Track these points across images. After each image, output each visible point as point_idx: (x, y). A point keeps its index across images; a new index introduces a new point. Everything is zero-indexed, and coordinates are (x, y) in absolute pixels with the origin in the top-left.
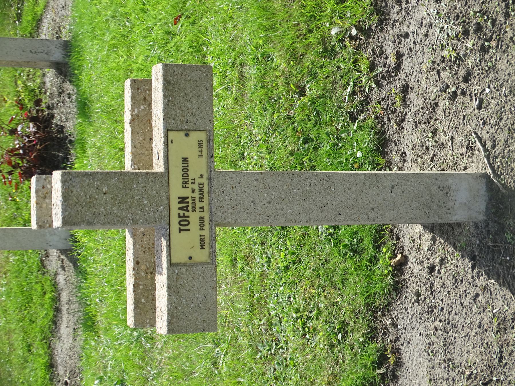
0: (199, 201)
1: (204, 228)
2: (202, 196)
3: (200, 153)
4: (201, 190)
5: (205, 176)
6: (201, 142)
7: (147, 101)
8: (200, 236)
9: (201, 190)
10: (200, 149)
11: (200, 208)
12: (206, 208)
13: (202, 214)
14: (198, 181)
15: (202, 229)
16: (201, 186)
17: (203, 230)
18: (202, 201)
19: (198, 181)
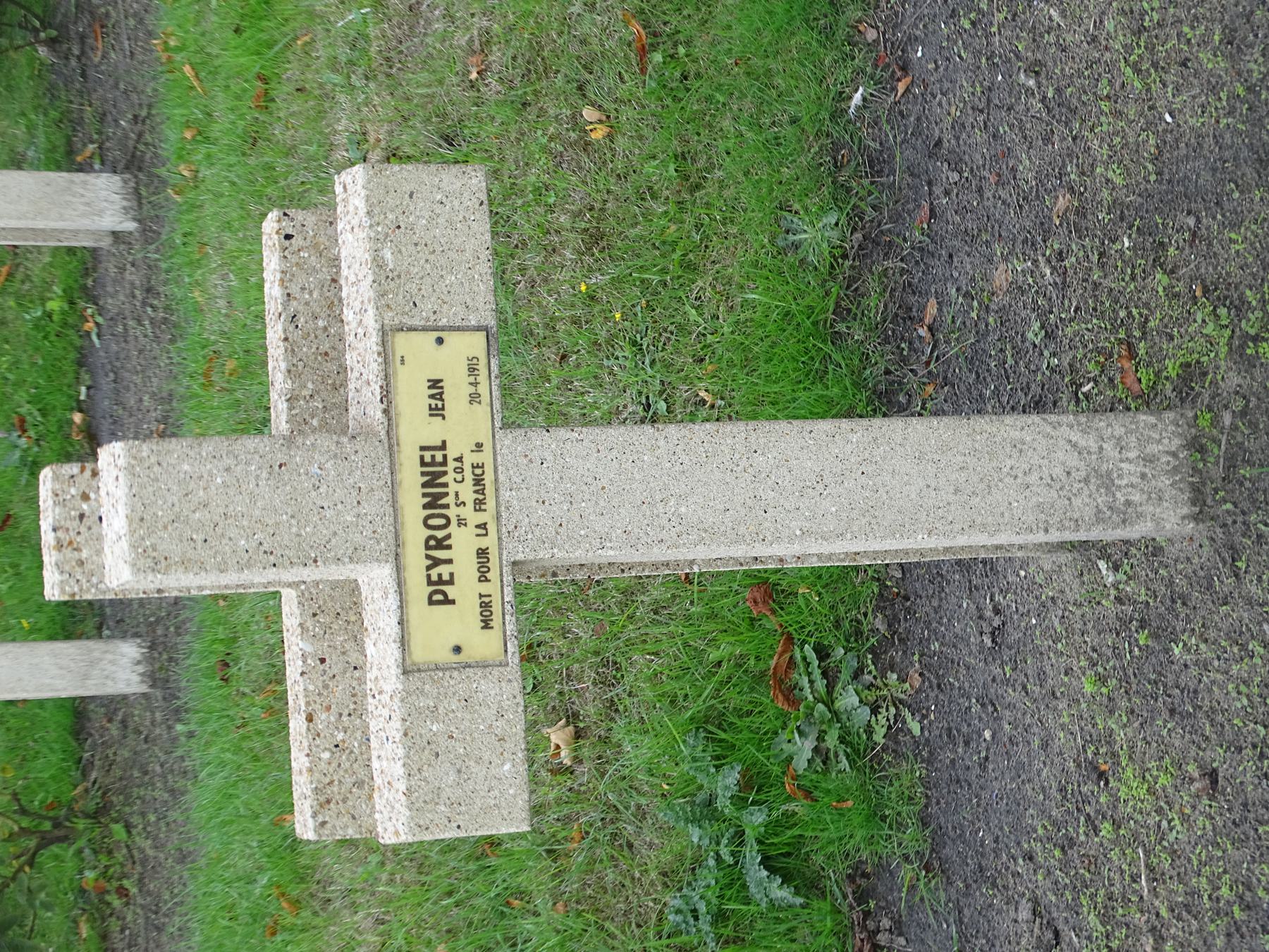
2: (481, 497)
3: (472, 389)
4: (478, 481)
5: (488, 447)
6: (475, 361)
8: (481, 596)
9: (478, 481)
10: (472, 379)
11: (477, 526)
12: (492, 528)
15: (483, 578)
16: (478, 471)
17: (487, 580)
18: (480, 510)
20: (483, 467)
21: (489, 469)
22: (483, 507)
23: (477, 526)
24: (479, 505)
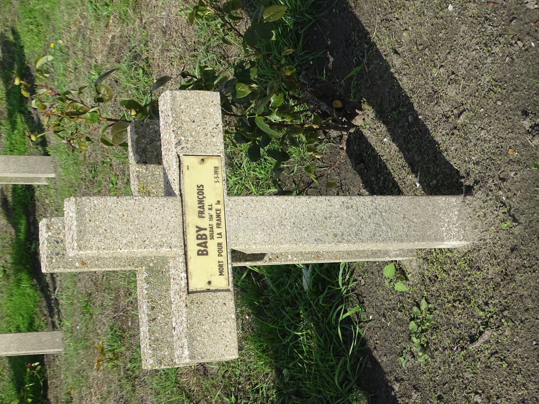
1: (222, 254)
2: (219, 222)
4: (218, 216)
5: (222, 202)
8: (219, 262)
9: (218, 216)
10: (216, 176)
11: (218, 234)
12: (224, 234)
13: (220, 240)
14: (215, 207)
15: (220, 255)
16: (218, 212)
17: (222, 256)
18: (219, 227)
19: (215, 207)
20: (220, 210)
23: (218, 234)
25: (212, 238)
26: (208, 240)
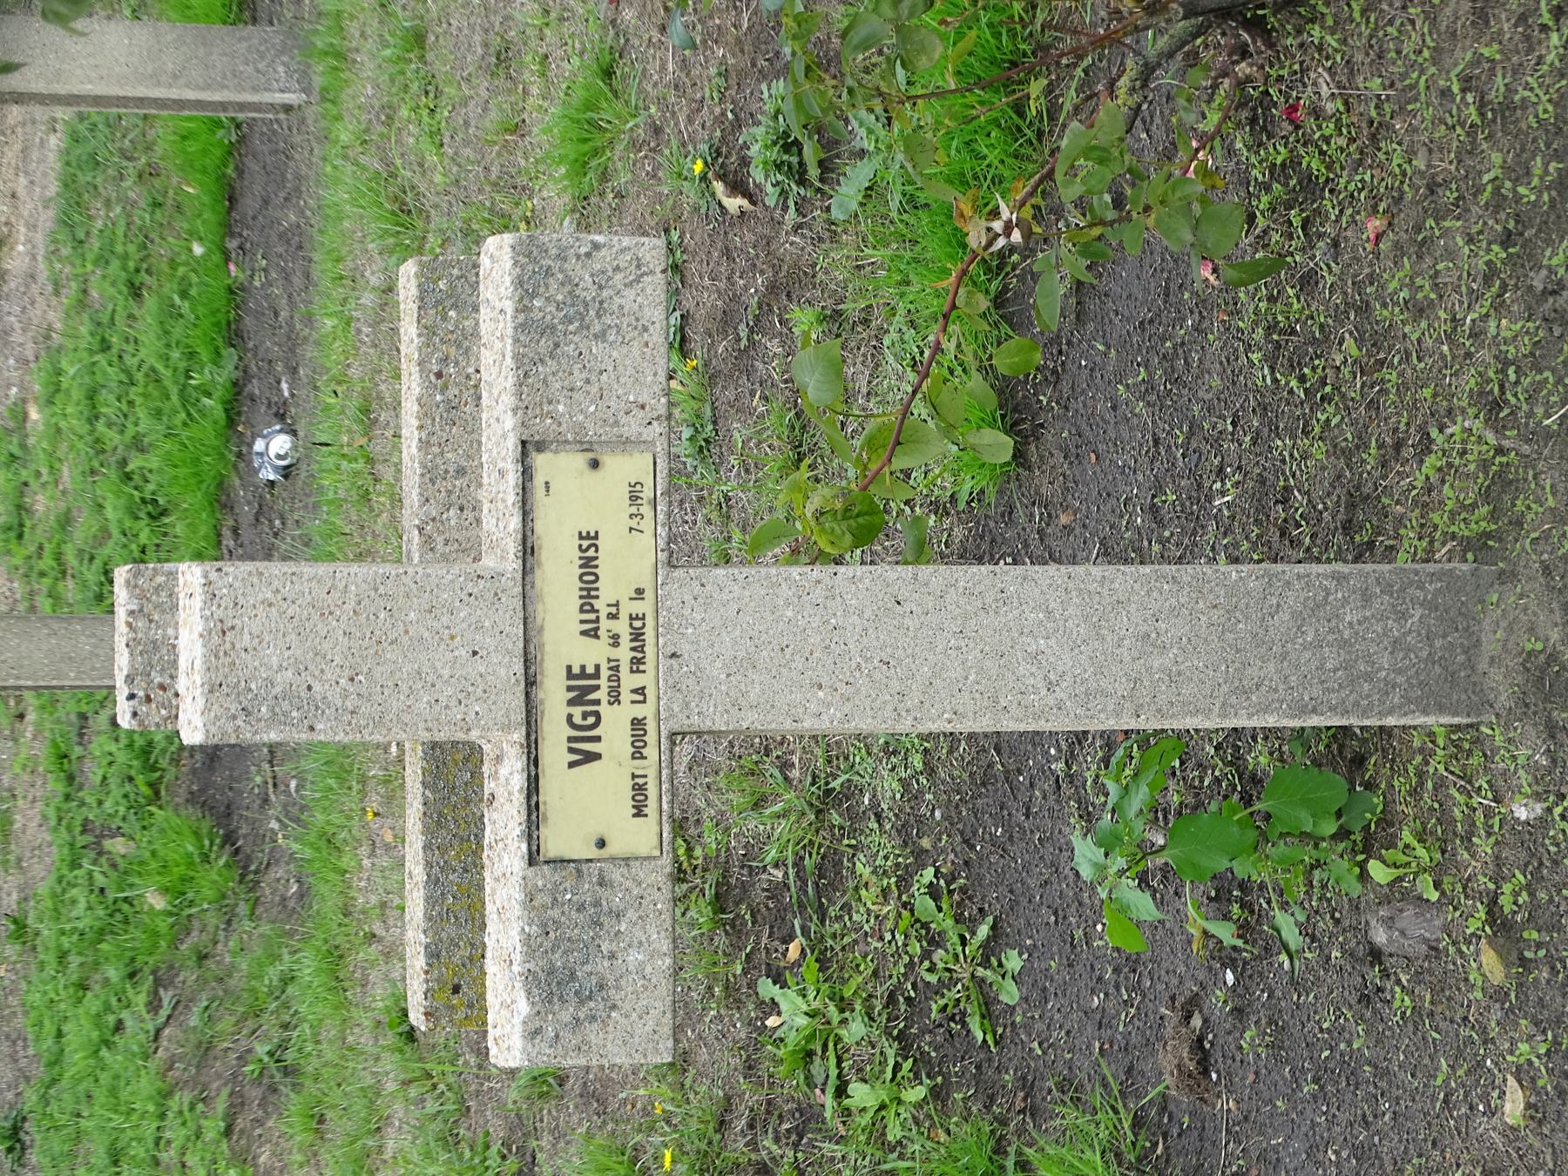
0: (632, 671)
1: (645, 752)
2: (639, 655)
4: (637, 635)
5: (649, 595)
7: (466, 341)
8: (634, 776)
9: (637, 635)
10: (634, 510)
11: (635, 691)
12: (650, 693)
13: (639, 711)
15: (638, 755)
16: (638, 624)
18: (638, 671)
19: (629, 607)
20: (643, 618)
21: (650, 622)
22: (642, 667)
23: (635, 691)
24: (637, 664)
25: (615, 698)
26: (604, 709)
